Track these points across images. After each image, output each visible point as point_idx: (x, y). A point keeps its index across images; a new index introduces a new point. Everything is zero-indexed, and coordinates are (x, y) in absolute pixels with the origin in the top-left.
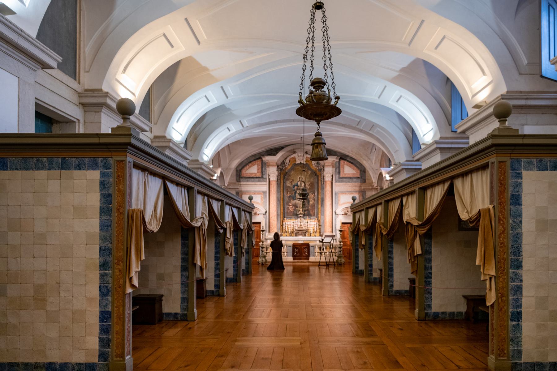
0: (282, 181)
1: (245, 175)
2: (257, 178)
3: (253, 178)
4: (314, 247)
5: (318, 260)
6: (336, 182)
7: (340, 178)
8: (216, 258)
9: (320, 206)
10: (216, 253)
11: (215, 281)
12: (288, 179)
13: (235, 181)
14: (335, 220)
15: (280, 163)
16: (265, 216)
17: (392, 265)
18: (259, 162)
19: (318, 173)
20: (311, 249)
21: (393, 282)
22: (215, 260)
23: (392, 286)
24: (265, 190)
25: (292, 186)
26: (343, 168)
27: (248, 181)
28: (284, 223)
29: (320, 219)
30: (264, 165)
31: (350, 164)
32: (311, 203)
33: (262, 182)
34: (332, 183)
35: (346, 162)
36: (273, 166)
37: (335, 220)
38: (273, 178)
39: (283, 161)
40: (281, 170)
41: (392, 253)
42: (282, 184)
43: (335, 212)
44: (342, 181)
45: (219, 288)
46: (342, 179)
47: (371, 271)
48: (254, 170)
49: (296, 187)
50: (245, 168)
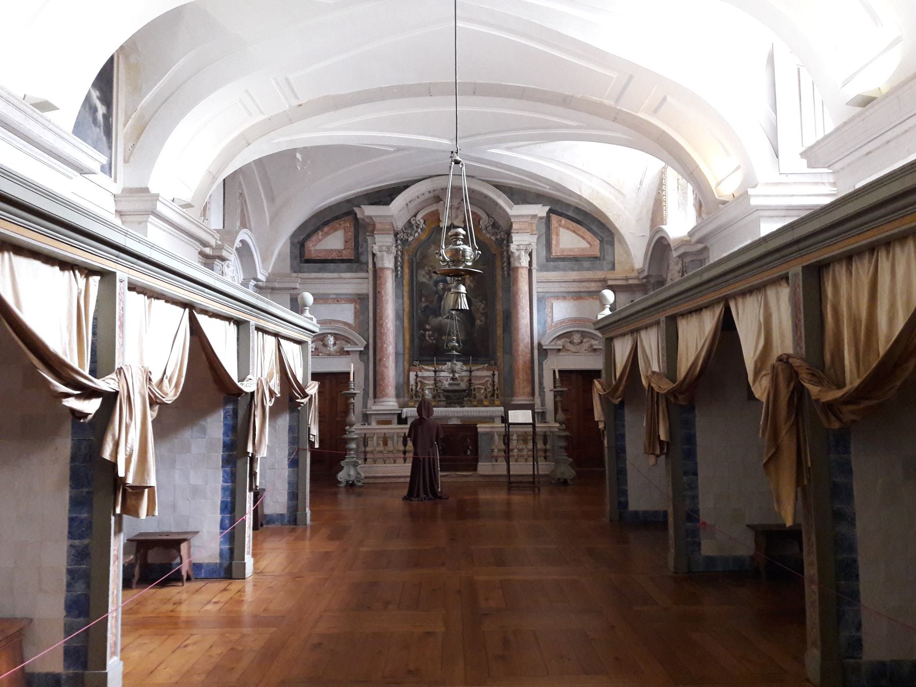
0: (406, 270)
1: (313, 256)
2: (343, 261)
3: (333, 261)
4: (490, 435)
5: (500, 468)
6: (542, 268)
7: (549, 259)
8: (77, 528)
9: (499, 331)
10: (76, 503)
11: (68, 630)
12: (420, 266)
13: (287, 269)
14: (541, 364)
15: (400, 224)
16: (366, 357)
17: (852, 548)
19: (494, 249)
20: (482, 443)
21: (859, 627)
22: (71, 535)
23: (857, 644)
24: (365, 291)
25: (431, 283)
26: (557, 235)
27: (319, 271)
28: (412, 375)
29: (500, 361)
30: (361, 230)
31: (575, 224)
32: (478, 322)
33: (356, 272)
34: (530, 271)
35: (564, 221)
36: (384, 232)
37: (541, 364)
38: (388, 262)
39: (409, 222)
40: (405, 242)
41: (850, 496)
42: (407, 277)
43: (540, 345)
44: (555, 269)
45: (85, 666)
46: (553, 261)
47: (694, 533)
48: (334, 242)
49: (441, 285)
50: (314, 238)
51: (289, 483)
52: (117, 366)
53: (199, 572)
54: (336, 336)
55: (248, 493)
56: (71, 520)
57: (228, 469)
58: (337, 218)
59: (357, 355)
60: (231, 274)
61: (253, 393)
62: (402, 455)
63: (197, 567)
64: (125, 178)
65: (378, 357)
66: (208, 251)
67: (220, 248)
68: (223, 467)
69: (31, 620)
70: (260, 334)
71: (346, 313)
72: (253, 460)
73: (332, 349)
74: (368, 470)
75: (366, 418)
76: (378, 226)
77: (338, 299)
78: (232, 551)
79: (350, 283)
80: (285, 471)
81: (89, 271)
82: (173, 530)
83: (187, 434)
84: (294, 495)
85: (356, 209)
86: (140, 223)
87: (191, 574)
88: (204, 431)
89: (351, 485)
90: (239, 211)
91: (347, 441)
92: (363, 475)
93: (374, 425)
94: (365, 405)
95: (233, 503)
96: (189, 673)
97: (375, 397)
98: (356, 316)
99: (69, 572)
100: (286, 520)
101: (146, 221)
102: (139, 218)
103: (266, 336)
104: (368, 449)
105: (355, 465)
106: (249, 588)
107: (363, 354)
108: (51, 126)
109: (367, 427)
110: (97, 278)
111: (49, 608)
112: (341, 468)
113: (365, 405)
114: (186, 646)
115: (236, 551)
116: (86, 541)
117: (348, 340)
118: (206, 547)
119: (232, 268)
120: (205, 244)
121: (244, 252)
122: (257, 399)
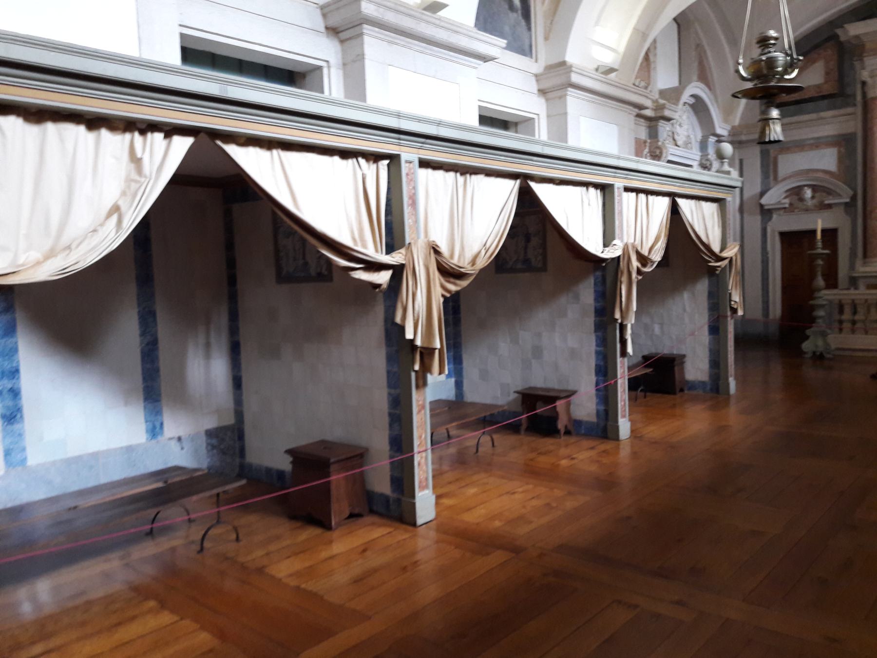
2: (824, 97)
18: (829, 51)
22: (390, 385)
24: (850, 130)
33: (840, 108)
51: (710, 350)
52: (407, 242)
53: (576, 429)
54: (815, 188)
55: (619, 360)
56: (388, 372)
57: (599, 334)
58: (816, 47)
59: (842, 207)
60: (686, 133)
61: (619, 257)
62: (836, 325)
63: (578, 423)
64: (544, 56)
65: (869, 209)
66: (648, 113)
67: (662, 107)
68: (596, 331)
69: (367, 450)
70: (642, 196)
71: (826, 160)
72: (623, 327)
73: (810, 203)
74: (835, 340)
75: (853, 282)
76: (868, 46)
77: (817, 144)
78: (606, 412)
79: (831, 123)
80: (705, 337)
81: (375, 157)
82: (556, 387)
83: (563, 300)
84: (717, 362)
85: (839, 32)
86: (560, 98)
87: (570, 428)
88: (577, 297)
89: (818, 357)
90: (695, 65)
91: (813, 308)
92: (833, 346)
93: (862, 289)
94: (852, 267)
95: (606, 367)
96: (493, 518)
97: (865, 256)
98: (841, 160)
99: (390, 414)
100: (708, 387)
101: (566, 95)
102: (559, 93)
103: (651, 198)
104: (857, 317)
105: (824, 335)
106: (625, 452)
107: (849, 207)
108: (442, 24)
109: (852, 291)
110: (386, 162)
111: (378, 441)
112: (807, 338)
113: (852, 267)
114: (514, 493)
115: (610, 413)
116: (398, 391)
117: (829, 192)
118: (585, 406)
119: (685, 127)
120: (640, 107)
121: (699, 107)
122: (623, 264)
